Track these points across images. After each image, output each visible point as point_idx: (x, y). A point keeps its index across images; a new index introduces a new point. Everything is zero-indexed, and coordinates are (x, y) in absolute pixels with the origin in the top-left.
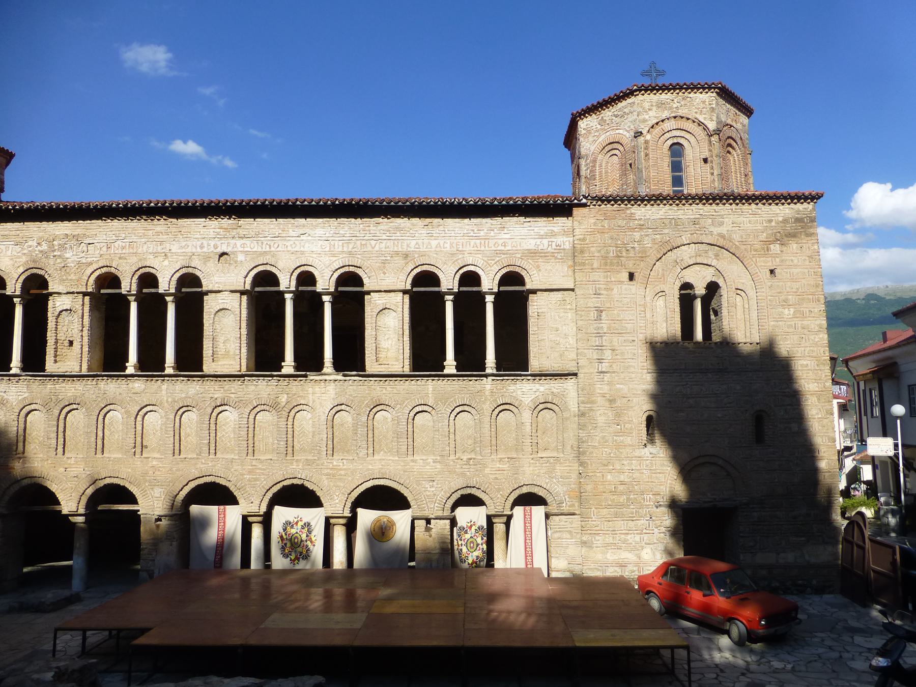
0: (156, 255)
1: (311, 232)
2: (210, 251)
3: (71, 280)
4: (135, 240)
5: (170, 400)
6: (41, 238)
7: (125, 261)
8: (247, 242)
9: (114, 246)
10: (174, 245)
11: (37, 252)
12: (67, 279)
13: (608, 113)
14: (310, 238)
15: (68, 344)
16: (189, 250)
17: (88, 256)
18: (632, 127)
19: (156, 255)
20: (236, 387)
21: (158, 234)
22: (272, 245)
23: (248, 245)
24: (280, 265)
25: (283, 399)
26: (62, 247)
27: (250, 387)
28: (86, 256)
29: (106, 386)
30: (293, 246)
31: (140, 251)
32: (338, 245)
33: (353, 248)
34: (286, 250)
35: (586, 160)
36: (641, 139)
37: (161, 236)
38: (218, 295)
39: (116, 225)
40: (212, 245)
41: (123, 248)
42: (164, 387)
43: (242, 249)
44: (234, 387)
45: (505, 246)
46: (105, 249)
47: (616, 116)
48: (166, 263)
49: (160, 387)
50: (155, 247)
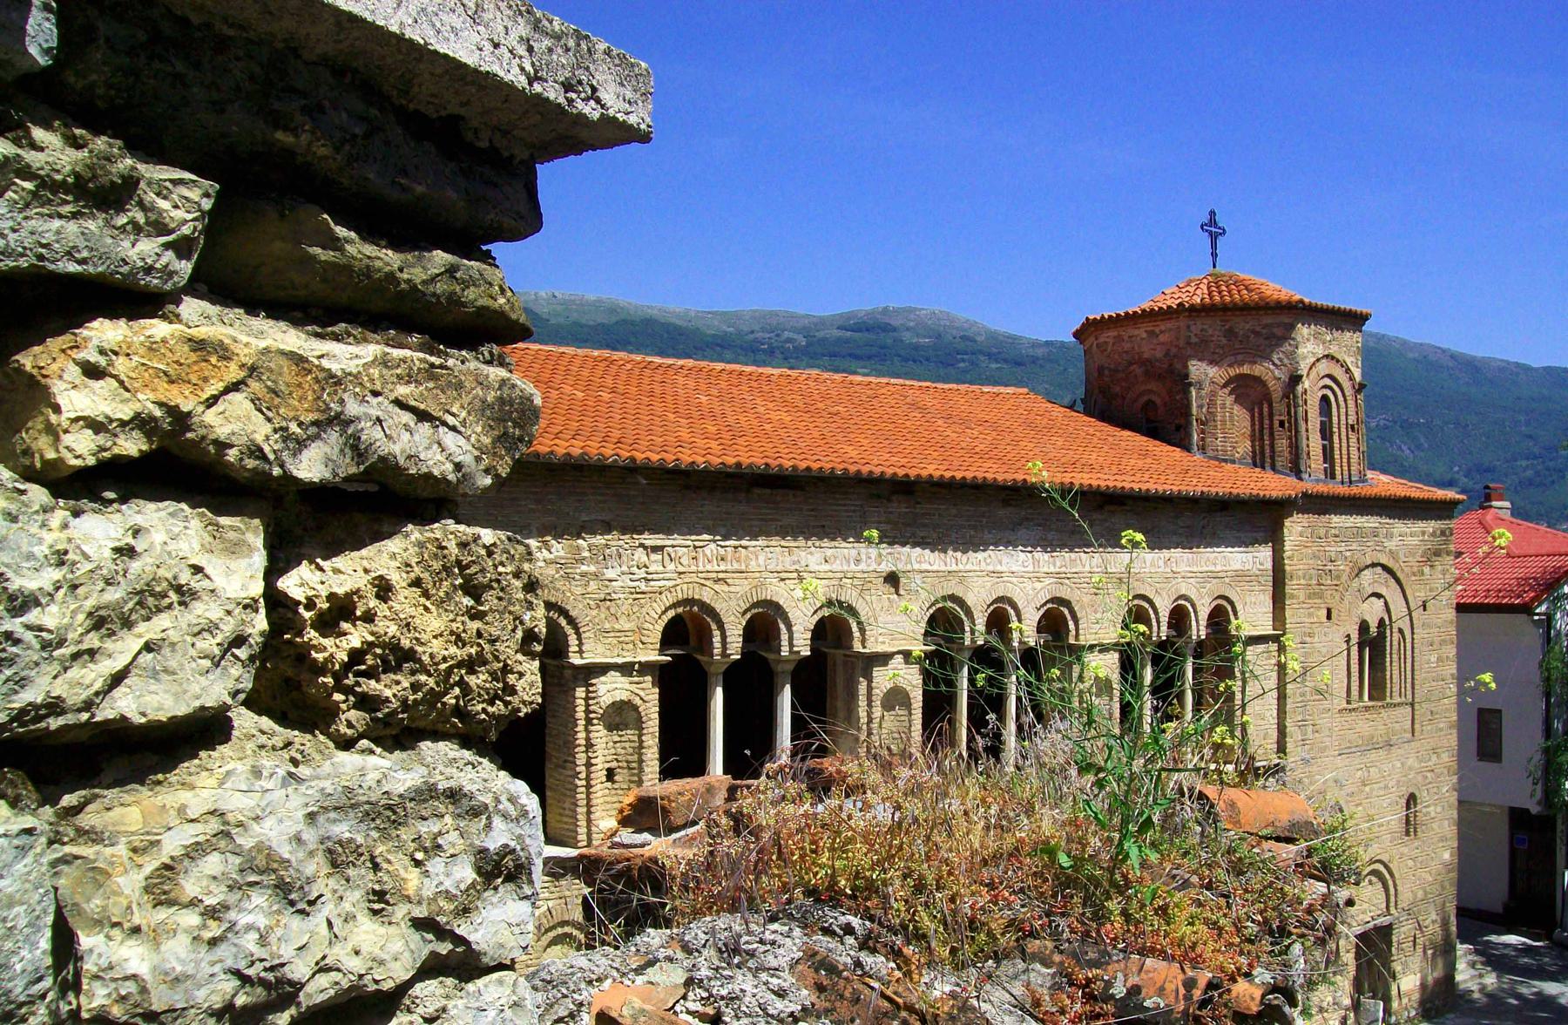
2: (871, 569)
7: (726, 588)
10: (811, 553)
13: (1243, 324)
15: (604, 779)
16: (836, 566)
17: (655, 576)
18: (1286, 361)
24: (970, 600)
28: (650, 577)
31: (753, 566)
35: (1201, 388)
36: (1300, 388)
43: (916, 566)
45: (1215, 564)
47: (1257, 334)
48: (799, 593)
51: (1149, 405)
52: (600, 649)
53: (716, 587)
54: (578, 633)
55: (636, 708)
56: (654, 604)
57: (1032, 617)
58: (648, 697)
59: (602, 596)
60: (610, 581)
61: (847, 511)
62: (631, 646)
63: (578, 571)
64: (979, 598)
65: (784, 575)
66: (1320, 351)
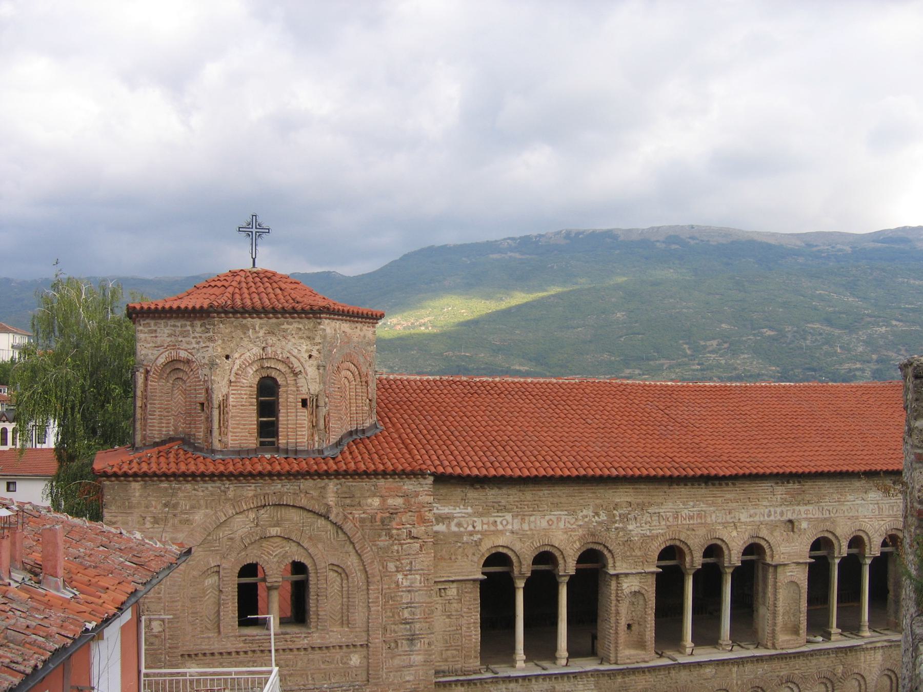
0: (725, 525)
1: (865, 496)
2: (777, 519)
3: (635, 556)
4: (704, 509)
5: (739, 682)
6: (597, 506)
7: (694, 533)
8: (810, 507)
9: (682, 516)
10: (742, 513)
11: (595, 524)
12: (631, 556)
14: (863, 502)
16: (757, 519)
19: (725, 525)
20: (800, 662)
21: (727, 501)
22: (831, 510)
23: (811, 511)
24: (838, 532)
25: (840, 669)
26: (624, 518)
27: (812, 661)
28: (652, 528)
29: (677, 675)
30: (849, 511)
31: (709, 520)
32: (886, 508)
33: (898, 511)
34: (842, 515)
37: (730, 504)
38: (786, 567)
39: (684, 491)
40: (778, 513)
41: (691, 518)
42: (735, 669)
43: (804, 516)
44: (798, 663)
46: (671, 519)
48: (734, 534)
49: (730, 670)
50: (724, 516)
52: (625, 565)
53: (688, 533)
54: (613, 557)
55: (643, 595)
56: (654, 543)
57: (877, 541)
59: (626, 539)
60: (630, 531)
61: (763, 489)
62: (641, 563)
63: (613, 527)
64: (843, 532)
65: (726, 525)
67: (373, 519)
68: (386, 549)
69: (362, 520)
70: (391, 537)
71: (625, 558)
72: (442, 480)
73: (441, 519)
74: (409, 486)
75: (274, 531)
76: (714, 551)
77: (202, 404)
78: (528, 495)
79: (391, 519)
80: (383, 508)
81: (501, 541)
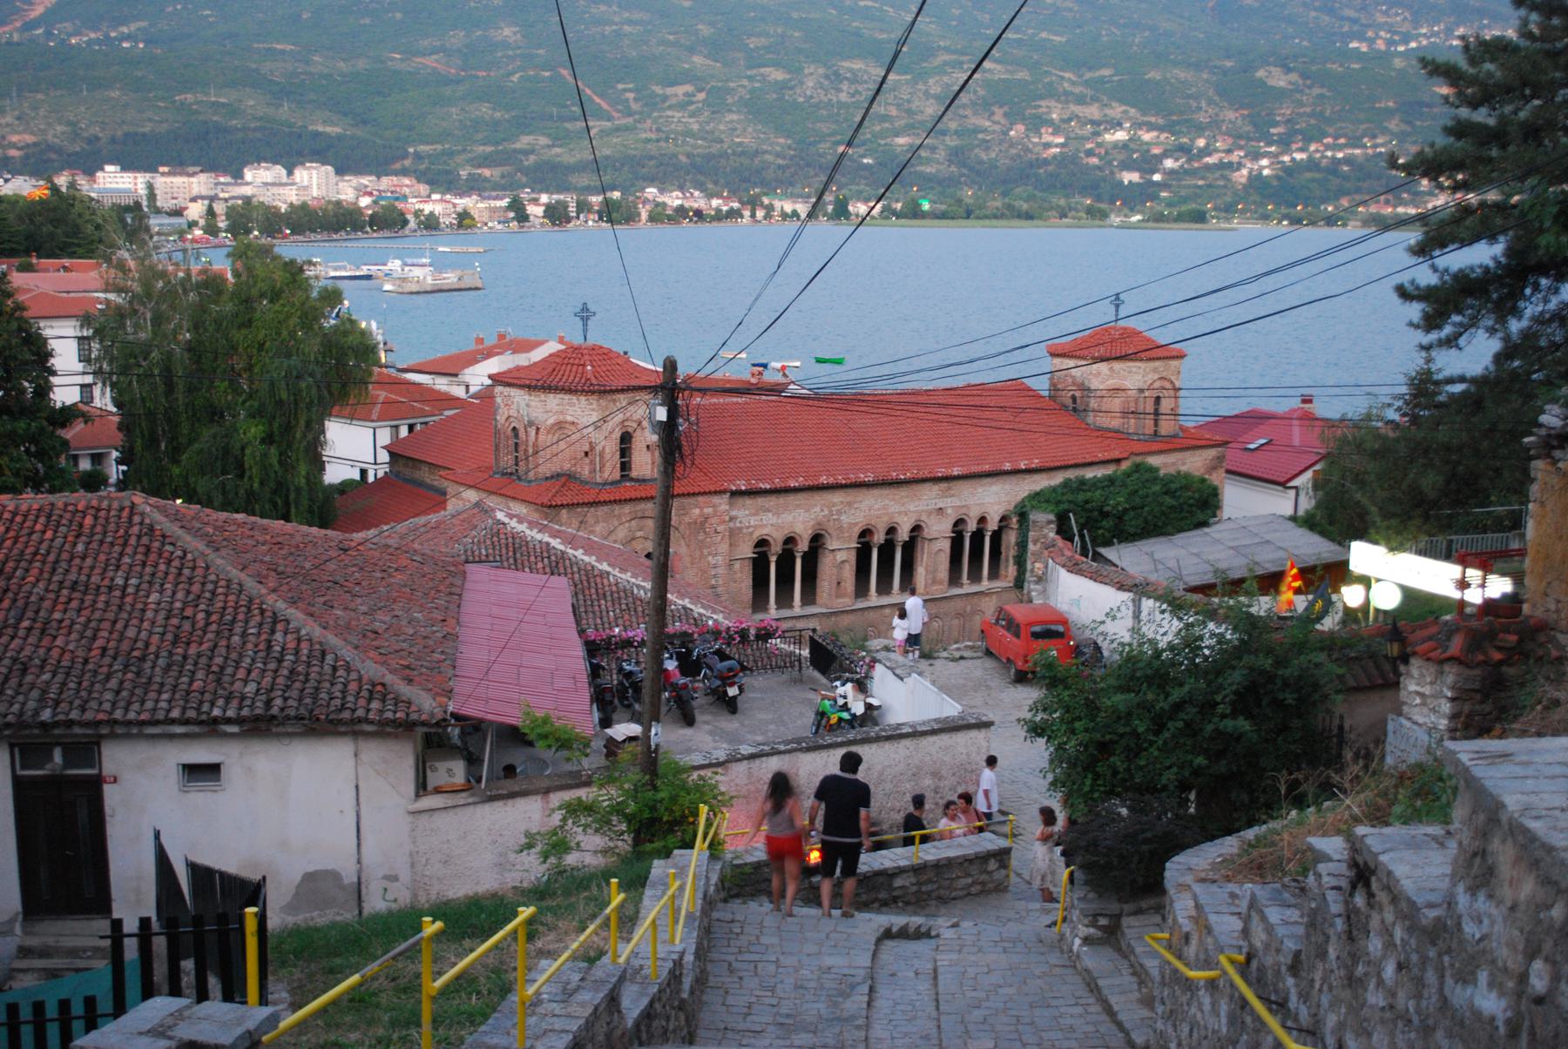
0: (900, 513)
24: (971, 515)
25: (968, 609)
26: (839, 512)
51: (1074, 398)
57: (997, 518)
58: (852, 557)
66: (1156, 377)
67: (696, 523)
68: (703, 541)
69: (689, 524)
70: (705, 532)
71: (839, 538)
72: (736, 494)
73: (732, 519)
74: (716, 500)
75: (639, 534)
76: (892, 530)
77: (586, 454)
78: (782, 500)
79: (705, 521)
80: (702, 515)
81: (765, 531)
